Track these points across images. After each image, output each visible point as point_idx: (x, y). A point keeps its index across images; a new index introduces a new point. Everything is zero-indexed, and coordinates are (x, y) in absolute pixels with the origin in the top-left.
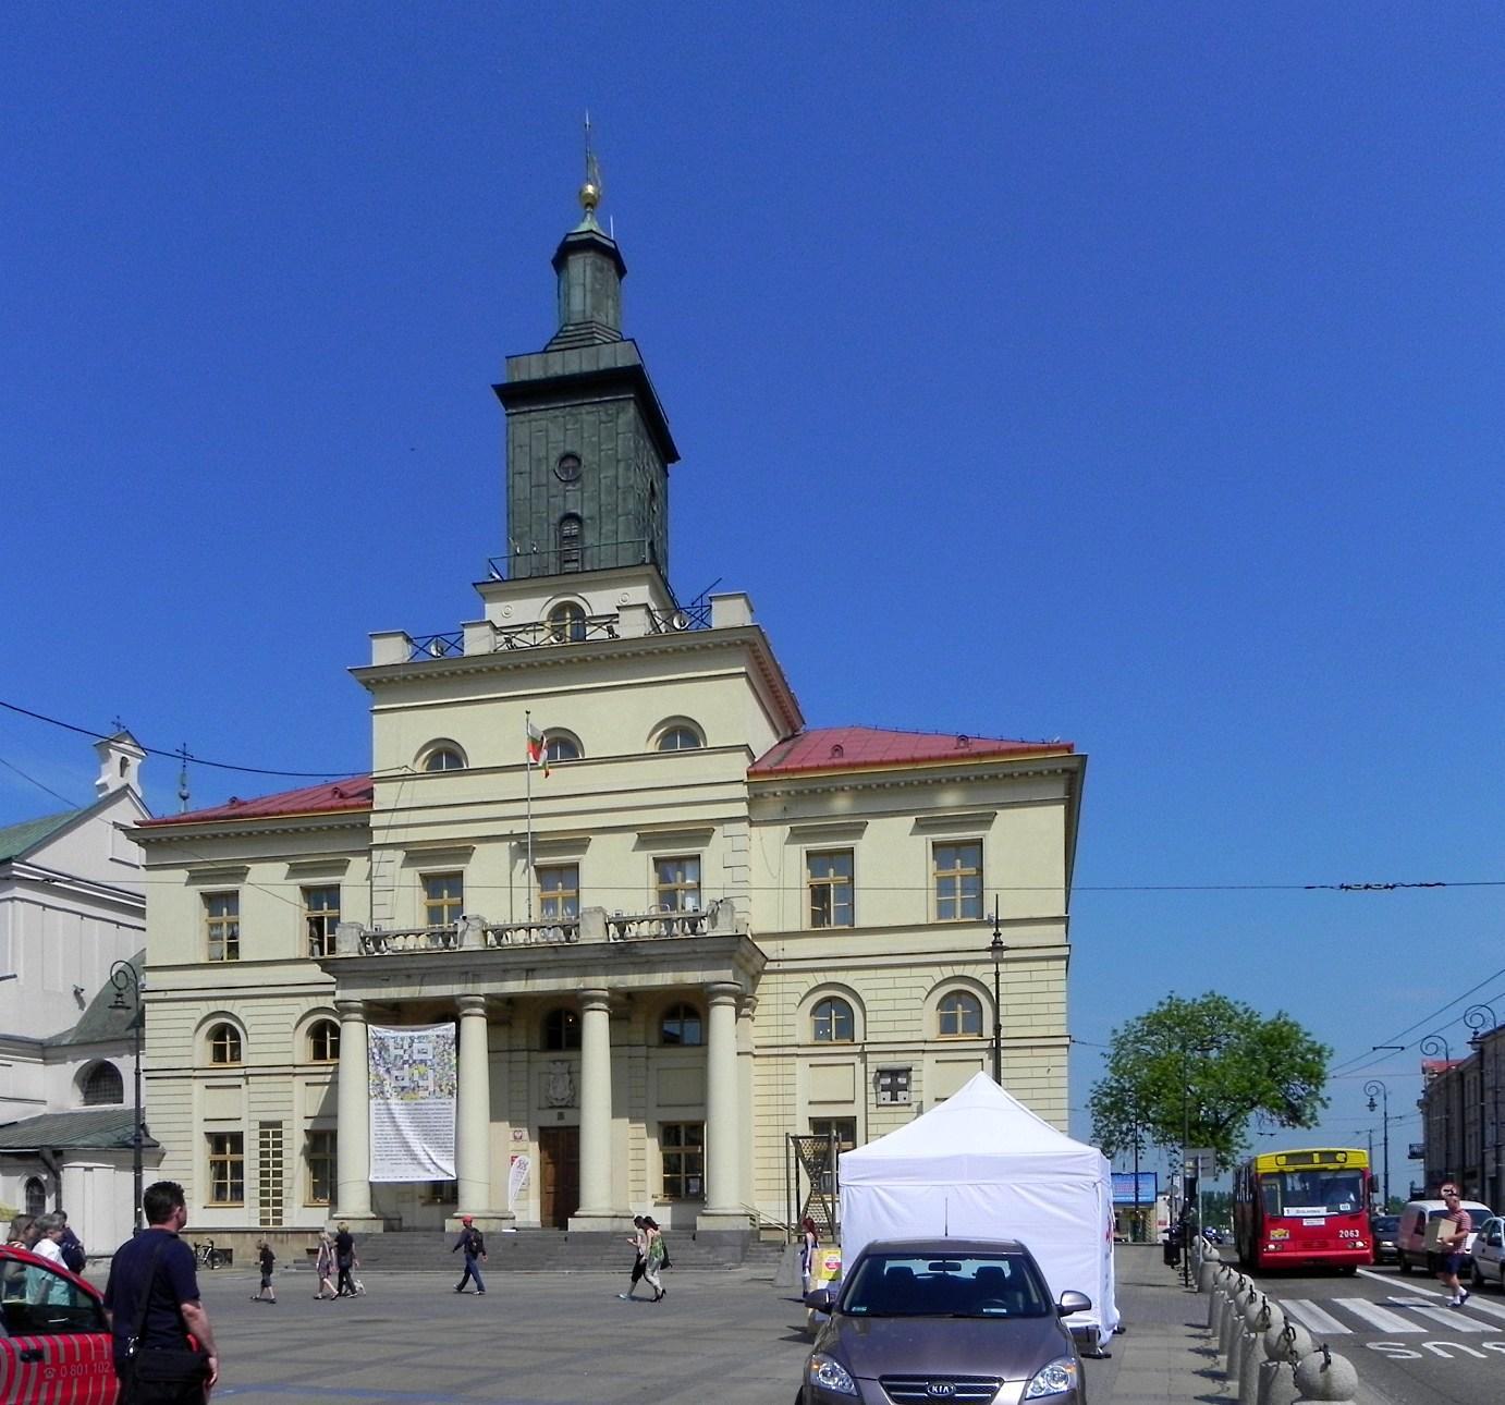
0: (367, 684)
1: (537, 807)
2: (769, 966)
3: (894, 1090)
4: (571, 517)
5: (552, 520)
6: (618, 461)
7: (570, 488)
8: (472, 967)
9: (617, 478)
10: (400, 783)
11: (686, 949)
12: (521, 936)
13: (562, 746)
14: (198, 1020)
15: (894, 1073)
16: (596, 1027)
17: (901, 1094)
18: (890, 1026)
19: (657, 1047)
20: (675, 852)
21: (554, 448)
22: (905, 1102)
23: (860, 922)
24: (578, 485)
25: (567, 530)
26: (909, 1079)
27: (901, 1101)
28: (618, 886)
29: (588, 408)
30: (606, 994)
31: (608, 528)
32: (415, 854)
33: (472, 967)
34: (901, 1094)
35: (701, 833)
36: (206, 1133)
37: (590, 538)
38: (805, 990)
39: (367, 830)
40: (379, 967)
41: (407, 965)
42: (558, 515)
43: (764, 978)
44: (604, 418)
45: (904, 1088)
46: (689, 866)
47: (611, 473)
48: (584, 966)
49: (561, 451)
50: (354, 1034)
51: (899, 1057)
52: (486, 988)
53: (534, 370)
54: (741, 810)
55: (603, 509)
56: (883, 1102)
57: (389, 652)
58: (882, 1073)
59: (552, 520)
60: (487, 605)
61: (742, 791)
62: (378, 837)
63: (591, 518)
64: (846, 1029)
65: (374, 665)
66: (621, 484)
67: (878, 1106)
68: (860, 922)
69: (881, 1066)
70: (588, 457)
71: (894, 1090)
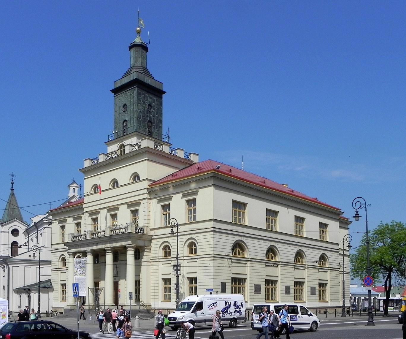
0: (84, 172)
1: (102, 202)
2: (153, 237)
6: (134, 104)
7: (125, 113)
8: (88, 243)
9: (133, 108)
10: (88, 196)
11: (121, 237)
13: (115, 183)
14: (58, 258)
21: (122, 103)
29: (128, 91)
30: (110, 248)
31: (132, 122)
32: (91, 213)
33: (88, 243)
35: (138, 203)
36: (61, 284)
37: (128, 126)
38: (160, 243)
39: (82, 209)
40: (73, 244)
42: (123, 120)
43: (153, 241)
44: (131, 93)
47: (132, 107)
48: (105, 242)
49: (123, 104)
50: (70, 260)
52: (90, 248)
53: (119, 84)
56: (175, 274)
57: (87, 164)
60: (108, 147)
61: (146, 191)
63: (129, 120)
66: (134, 110)
70: (128, 105)
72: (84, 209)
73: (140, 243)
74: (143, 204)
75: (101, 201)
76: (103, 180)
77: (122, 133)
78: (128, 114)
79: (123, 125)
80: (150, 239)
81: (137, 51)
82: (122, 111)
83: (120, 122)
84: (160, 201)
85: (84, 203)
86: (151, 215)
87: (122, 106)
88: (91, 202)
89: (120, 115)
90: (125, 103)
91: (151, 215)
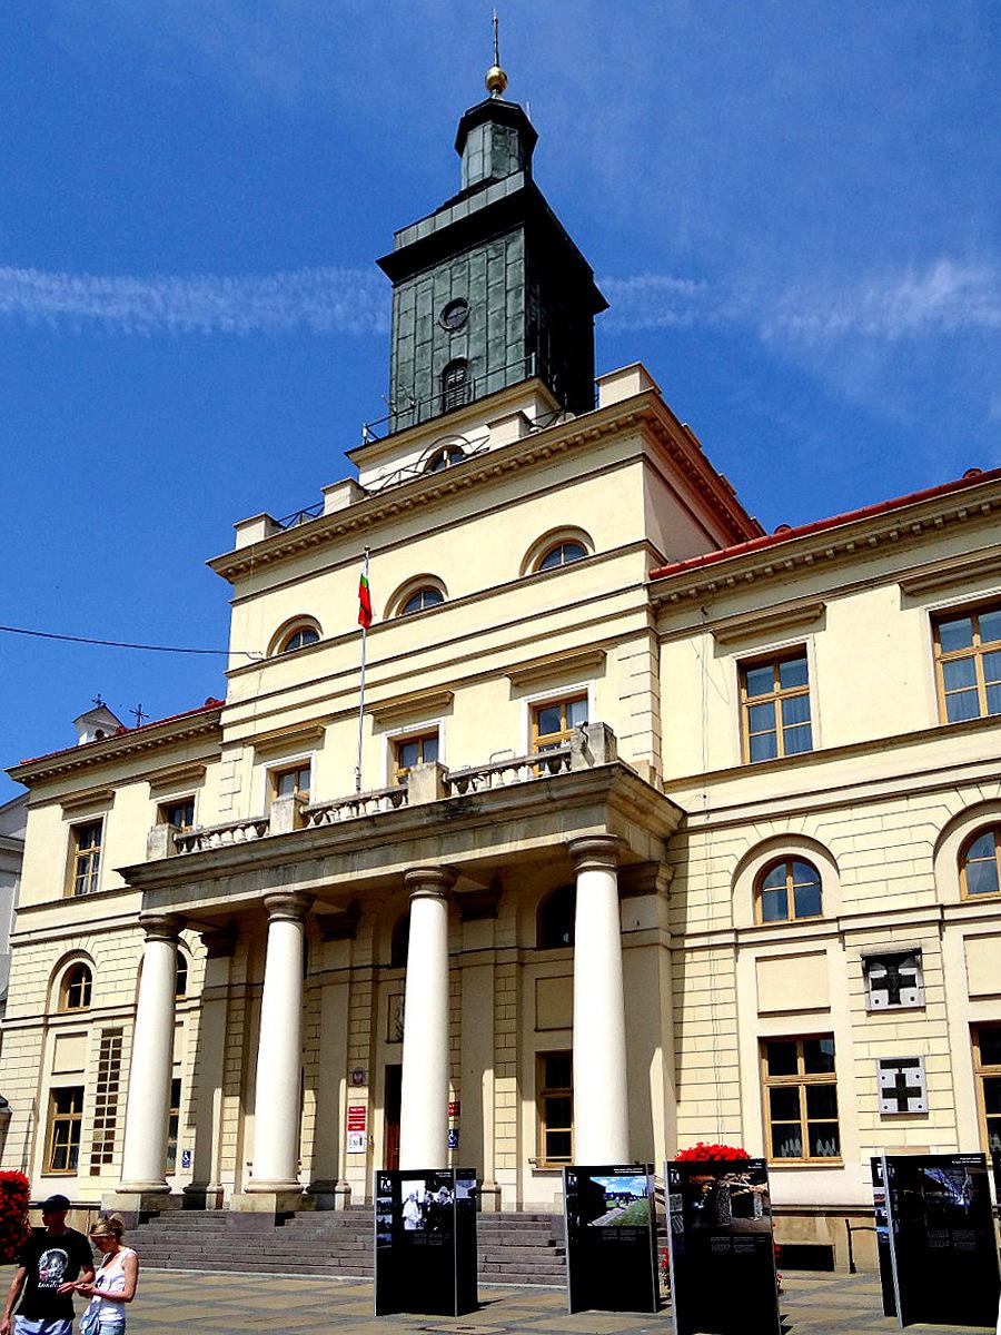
2: (692, 822)
3: (893, 985)
4: (460, 364)
5: (436, 373)
7: (455, 334)
12: (345, 814)
15: (892, 960)
16: (427, 919)
17: (905, 993)
18: (880, 889)
19: (535, 949)
20: (553, 685)
21: (439, 302)
22: (913, 1004)
23: (822, 740)
24: (465, 329)
25: (451, 379)
26: (919, 965)
27: (905, 1002)
28: (487, 734)
34: (905, 993)
37: (476, 374)
40: (180, 871)
41: (211, 865)
42: (442, 366)
45: (910, 982)
46: (576, 708)
51: (897, 934)
54: (641, 621)
55: (490, 345)
58: (870, 962)
59: (436, 373)
62: (229, 735)
64: (810, 904)
65: (237, 549)
67: (870, 1013)
68: (822, 740)
69: (869, 950)
70: (475, 298)
71: (893, 985)
72: (225, 731)
73: (642, 845)
74: (626, 665)
75: (360, 665)
76: (328, 598)
77: (456, 392)
78: (472, 337)
79: (444, 381)
80: (676, 835)
81: (502, 133)
82: (439, 330)
83: (425, 374)
84: (724, 642)
85: (227, 704)
86: (675, 711)
87: (438, 313)
88: (260, 694)
89: (423, 352)
90: (454, 297)
91: (675, 711)
